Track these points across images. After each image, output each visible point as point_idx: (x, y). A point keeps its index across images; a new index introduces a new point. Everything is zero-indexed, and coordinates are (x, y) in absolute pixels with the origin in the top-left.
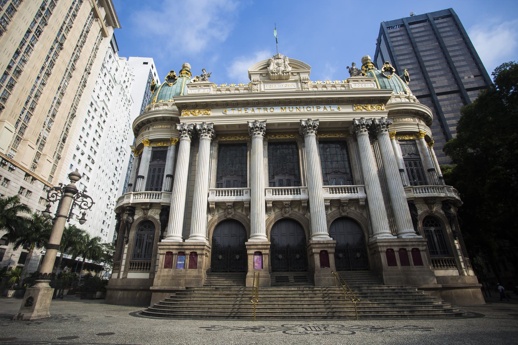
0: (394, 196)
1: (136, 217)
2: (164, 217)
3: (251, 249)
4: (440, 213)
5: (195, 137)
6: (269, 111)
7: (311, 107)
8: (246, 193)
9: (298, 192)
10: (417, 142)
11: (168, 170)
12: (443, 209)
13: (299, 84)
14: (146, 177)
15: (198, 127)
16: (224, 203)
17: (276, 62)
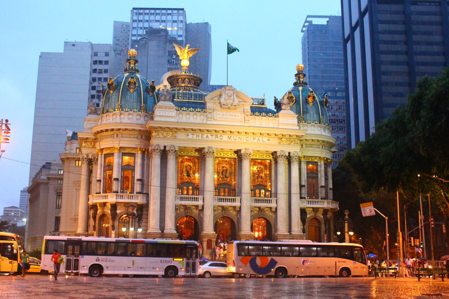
0: (293, 207)
1: (118, 212)
2: (139, 212)
3: (206, 238)
4: (320, 217)
5: (164, 154)
6: (219, 138)
7: (249, 137)
8: (200, 200)
9: (234, 200)
10: (319, 164)
11: (138, 175)
12: (323, 214)
13: (243, 115)
14: (120, 179)
15: (167, 149)
16: (185, 207)
17: (227, 93)
